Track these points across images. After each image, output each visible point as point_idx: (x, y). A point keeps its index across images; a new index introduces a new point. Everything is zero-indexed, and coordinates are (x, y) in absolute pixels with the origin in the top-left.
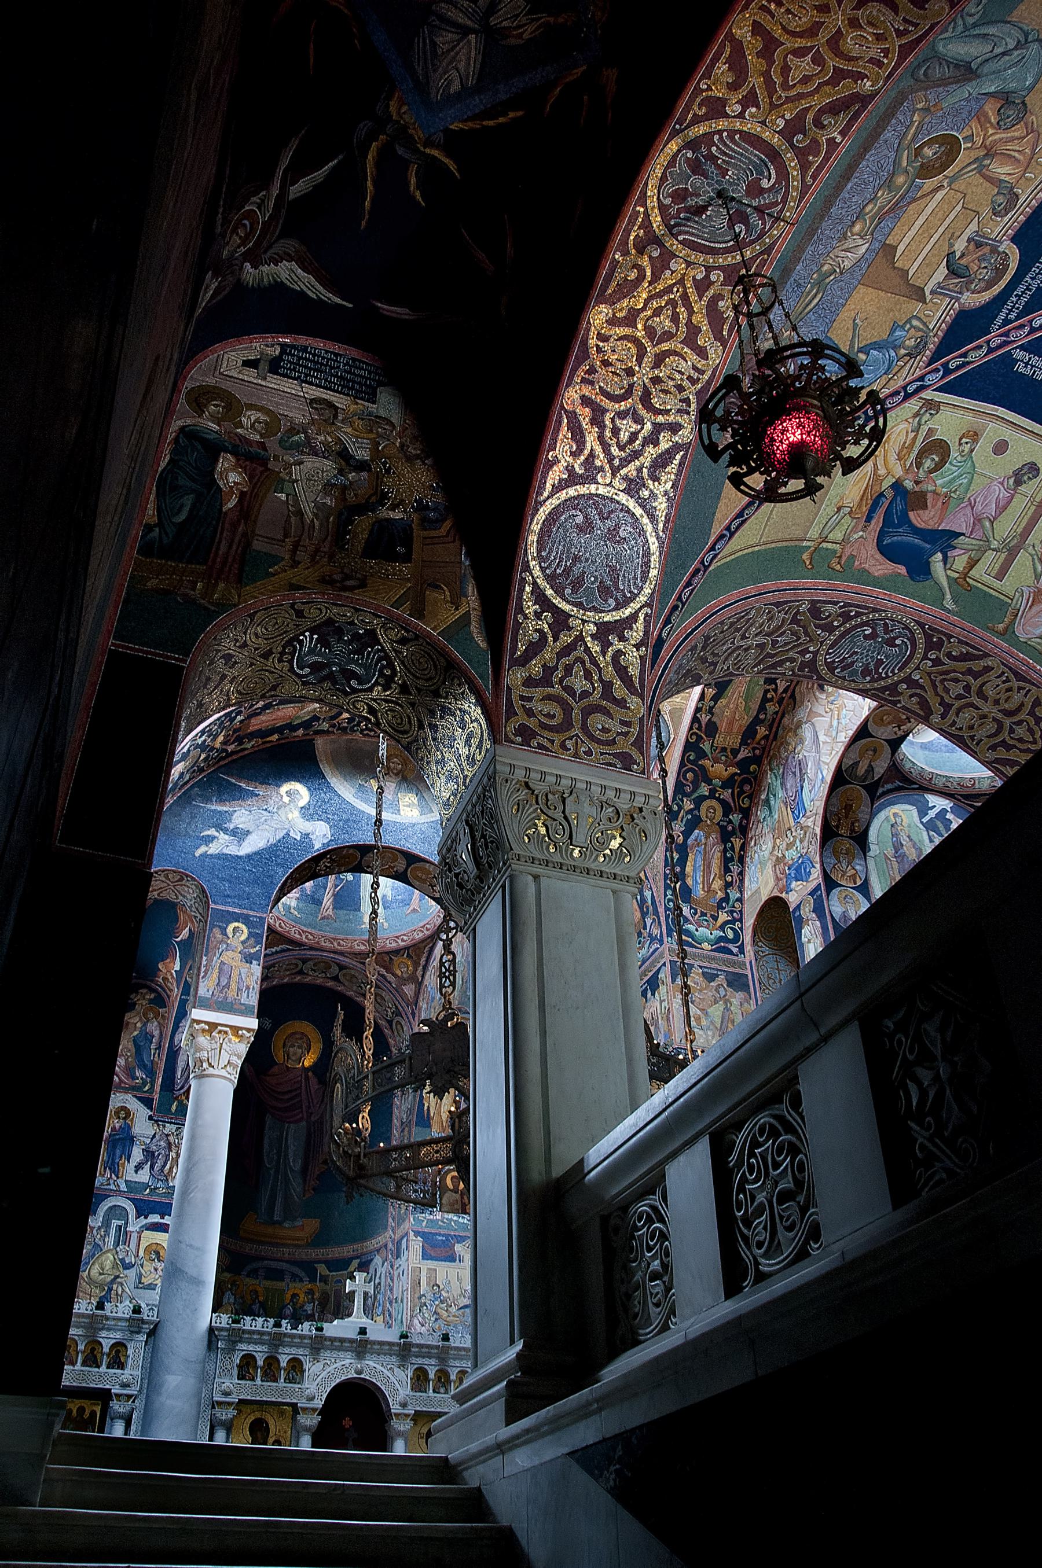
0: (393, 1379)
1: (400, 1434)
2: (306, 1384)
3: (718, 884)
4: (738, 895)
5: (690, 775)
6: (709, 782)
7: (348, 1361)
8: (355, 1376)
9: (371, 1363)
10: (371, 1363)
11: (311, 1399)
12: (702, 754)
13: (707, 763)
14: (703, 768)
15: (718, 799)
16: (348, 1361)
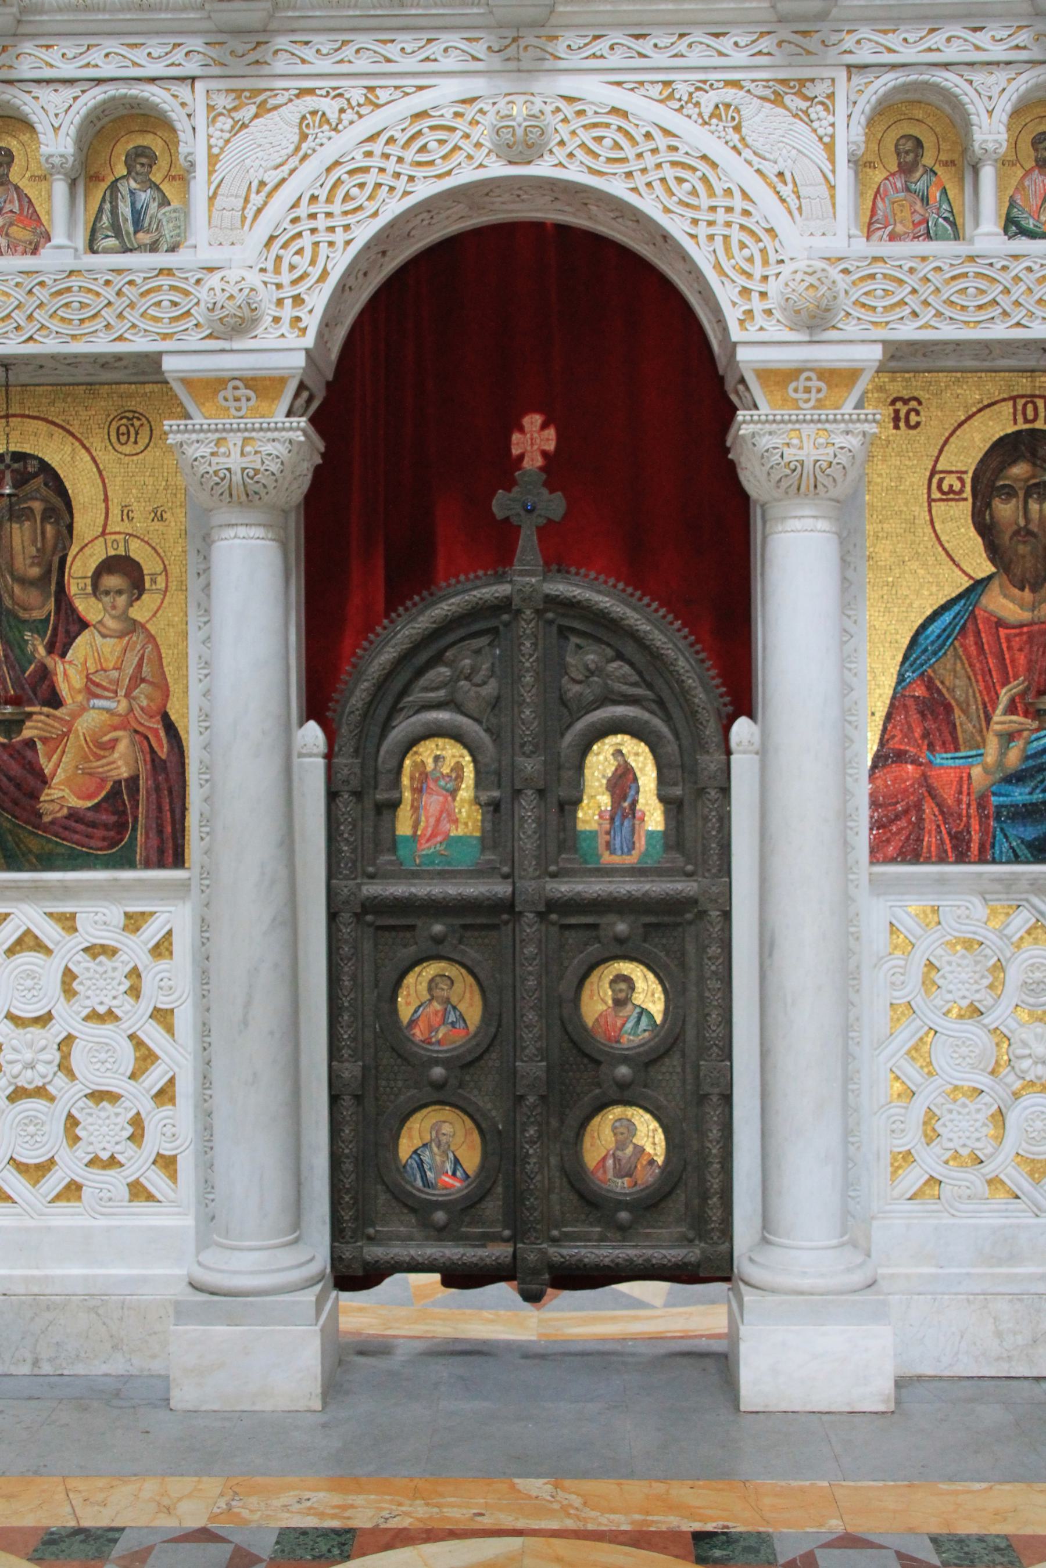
0: (736, 170)
1: (803, 483)
2: (201, 246)
7: (449, 90)
8: (498, 169)
9: (595, 90)
10: (595, 90)
11: (237, 324)
16: (449, 90)
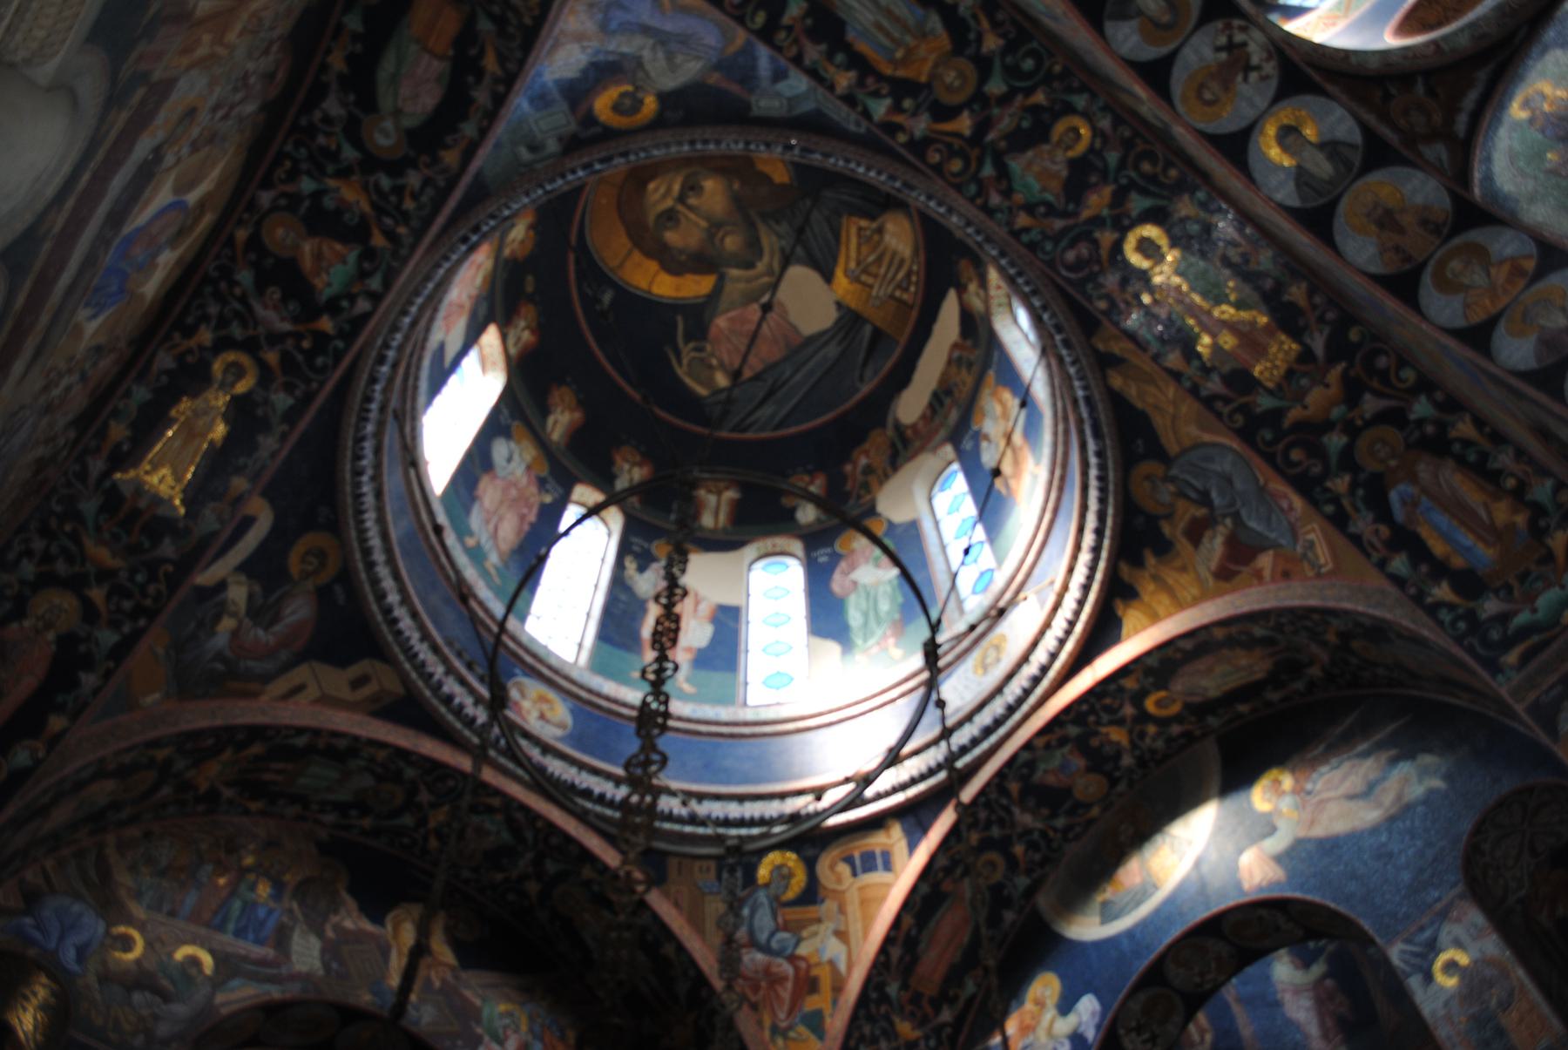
3: (1502, 512)
4: (1549, 483)
5: (1296, 455)
6: (1328, 426)
12: (1275, 415)
13: (1295, 414)
14: (1299, 426)
15: (1369, 424)
